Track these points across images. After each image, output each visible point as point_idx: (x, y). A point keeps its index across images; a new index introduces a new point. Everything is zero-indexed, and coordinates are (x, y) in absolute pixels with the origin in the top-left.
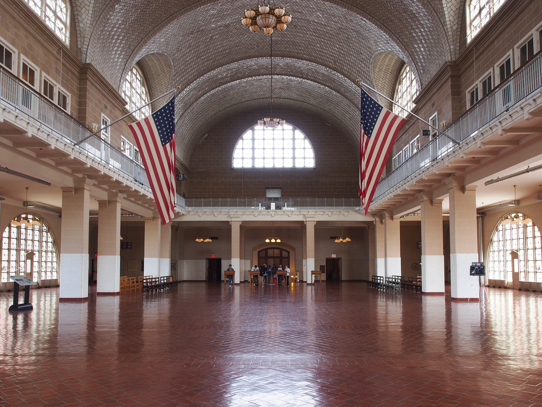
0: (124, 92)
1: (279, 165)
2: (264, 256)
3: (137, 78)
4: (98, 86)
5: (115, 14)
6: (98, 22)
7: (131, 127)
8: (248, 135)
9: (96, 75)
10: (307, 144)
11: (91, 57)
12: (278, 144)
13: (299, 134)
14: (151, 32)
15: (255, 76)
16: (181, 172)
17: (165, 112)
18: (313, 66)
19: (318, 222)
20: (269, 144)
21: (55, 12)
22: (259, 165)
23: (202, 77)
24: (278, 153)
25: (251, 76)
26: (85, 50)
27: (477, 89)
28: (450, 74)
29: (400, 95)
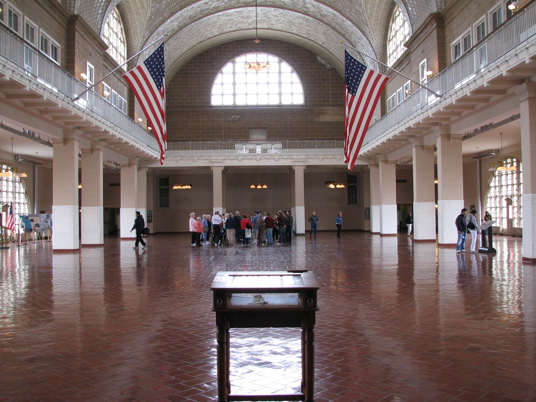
3: (114, 17)
8: (228, 68)
10: (295, 78)
13: (286, 67)
19: (307, 166)
22: (241, 101)
27: (459, 44)
28: (435, 25)
29: (393, 33)
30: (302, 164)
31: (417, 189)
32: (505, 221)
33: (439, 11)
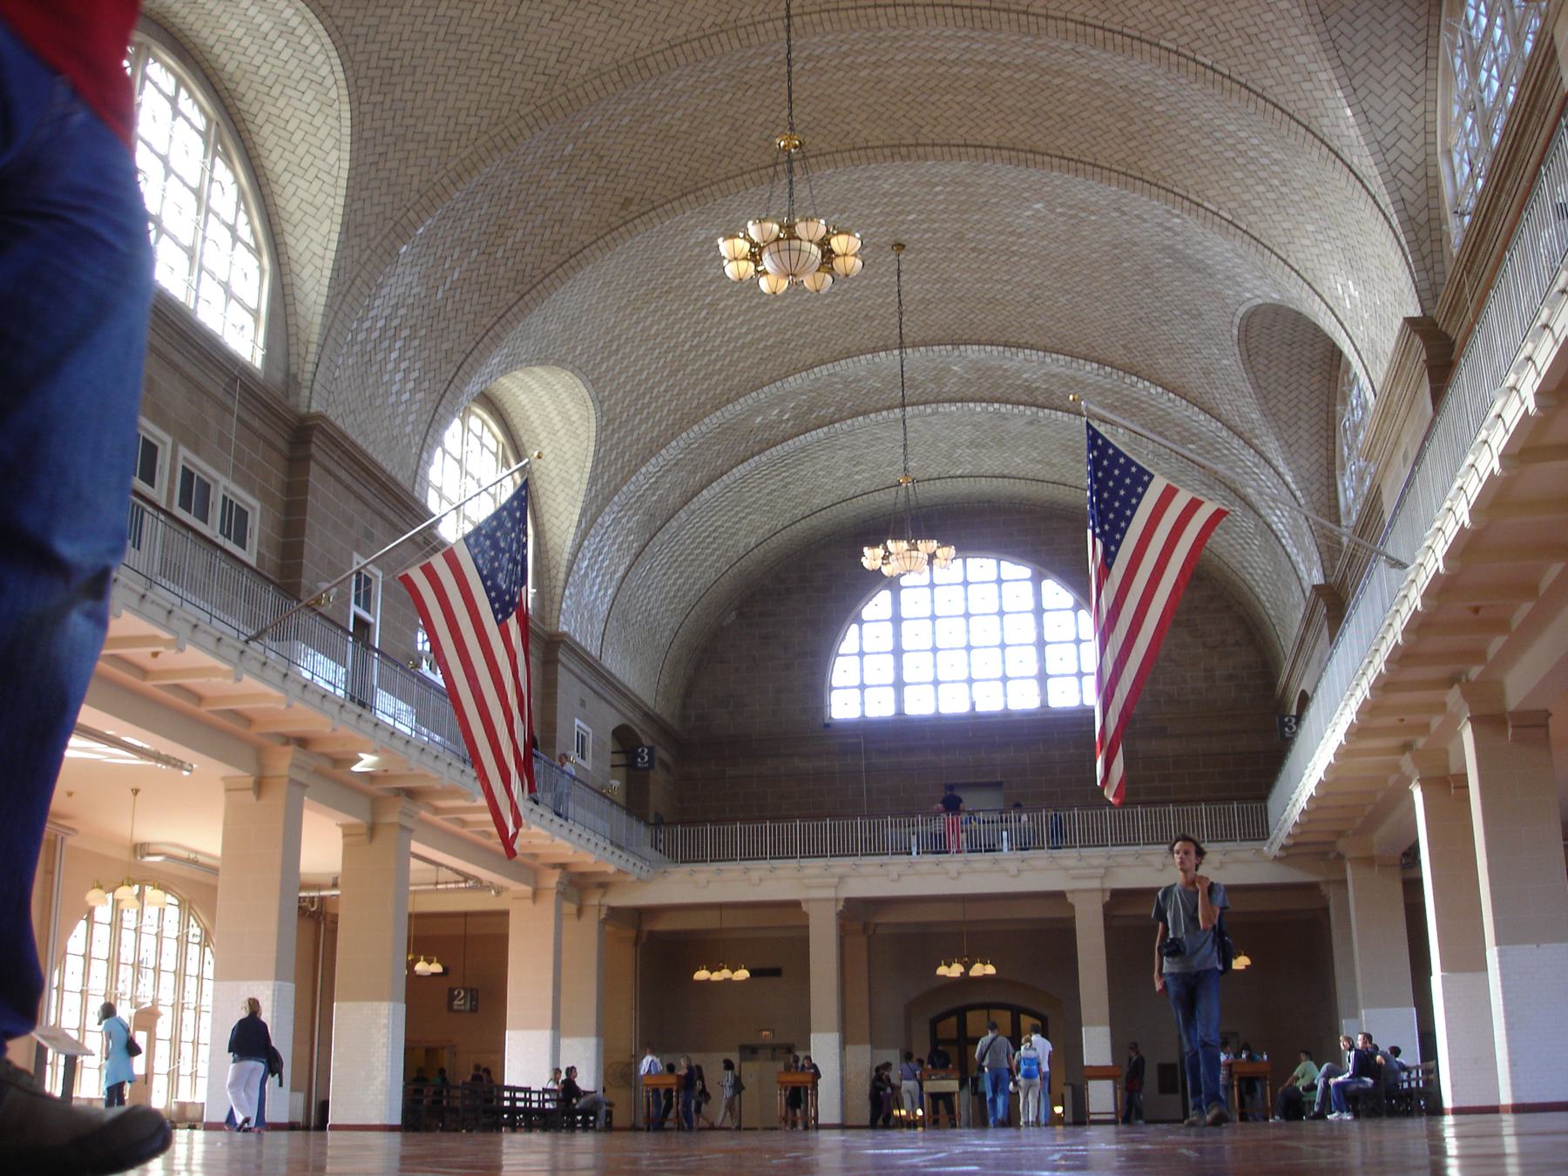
0: (439, 490)
1: (990, 702)
2: (954, 1035)
3: (483, 445)
4: (343, 475)
5: (399, 270)
6: (349, 298)
7: (407, 581)
9: (337, 445)
11: (325, 394)
12: (985, 631)
14: (515, 309)
15: (878, 411)
16: (646, 741)
18: (1058, 364)
20: (950, 634)
21: (226, 286)
22: (919, 705)
23: (696, 428)
24: (986, 663)
25: (865, 413)
26: (308, 376)
30: (1096, 884)
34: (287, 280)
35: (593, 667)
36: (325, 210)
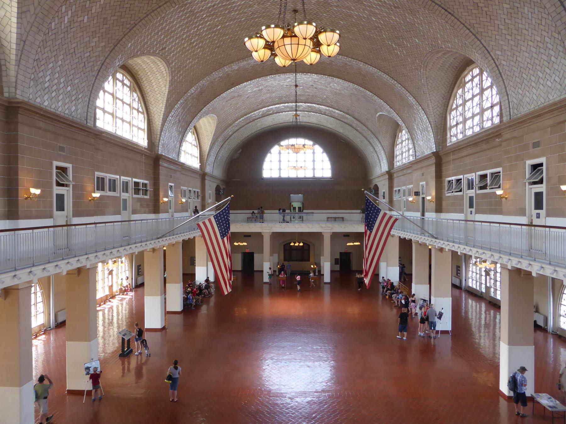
1: (301, 174)
7: (198, 225)
8: (275, 149)
13: (318, 149)
17: (223, 214)
19: (333, 233)
22: (284, 175)
30: (329, 231)
31: (416, 256)
32: (483, 286)
33: (438, 150)
34: (150, 118)
35: (212, 176)
36: (161, 101)
